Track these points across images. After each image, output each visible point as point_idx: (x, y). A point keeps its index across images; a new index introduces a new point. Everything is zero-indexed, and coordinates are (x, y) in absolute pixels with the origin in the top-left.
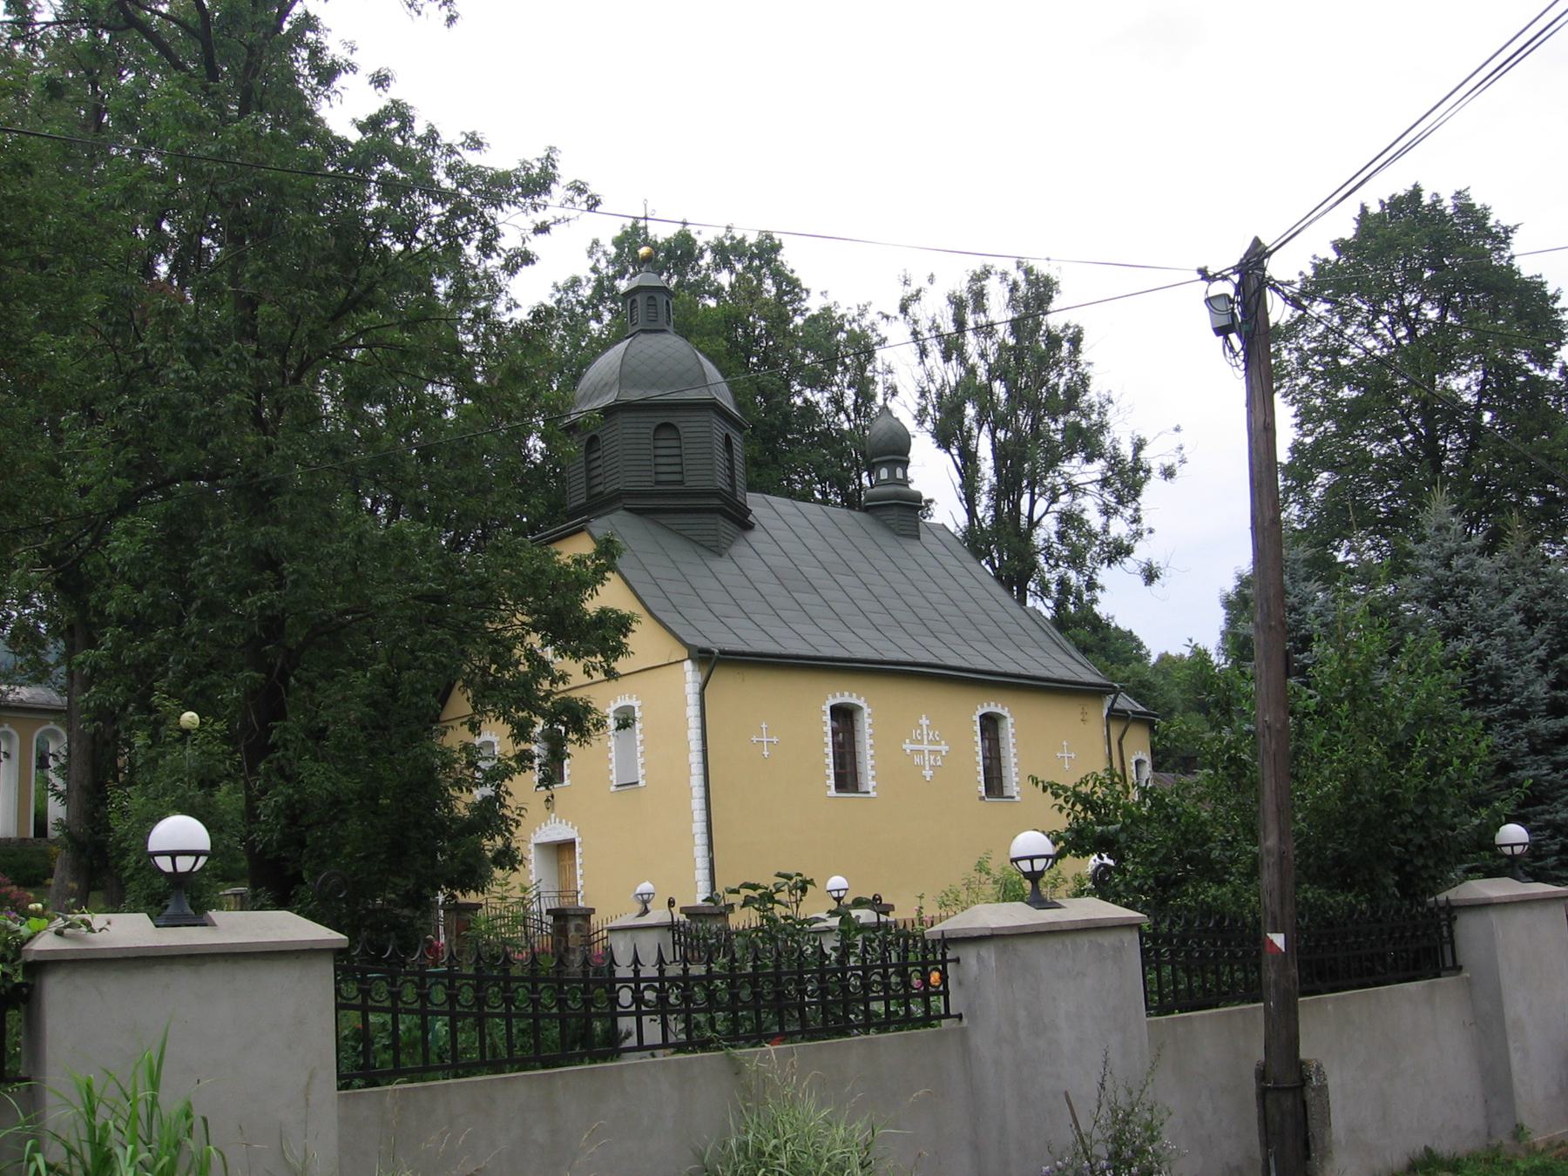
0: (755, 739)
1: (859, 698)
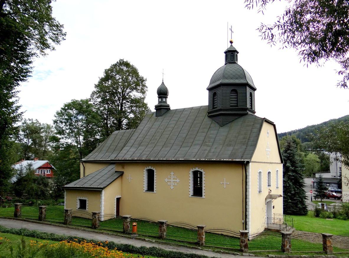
0: (127, 178)
1: (153, 168)
